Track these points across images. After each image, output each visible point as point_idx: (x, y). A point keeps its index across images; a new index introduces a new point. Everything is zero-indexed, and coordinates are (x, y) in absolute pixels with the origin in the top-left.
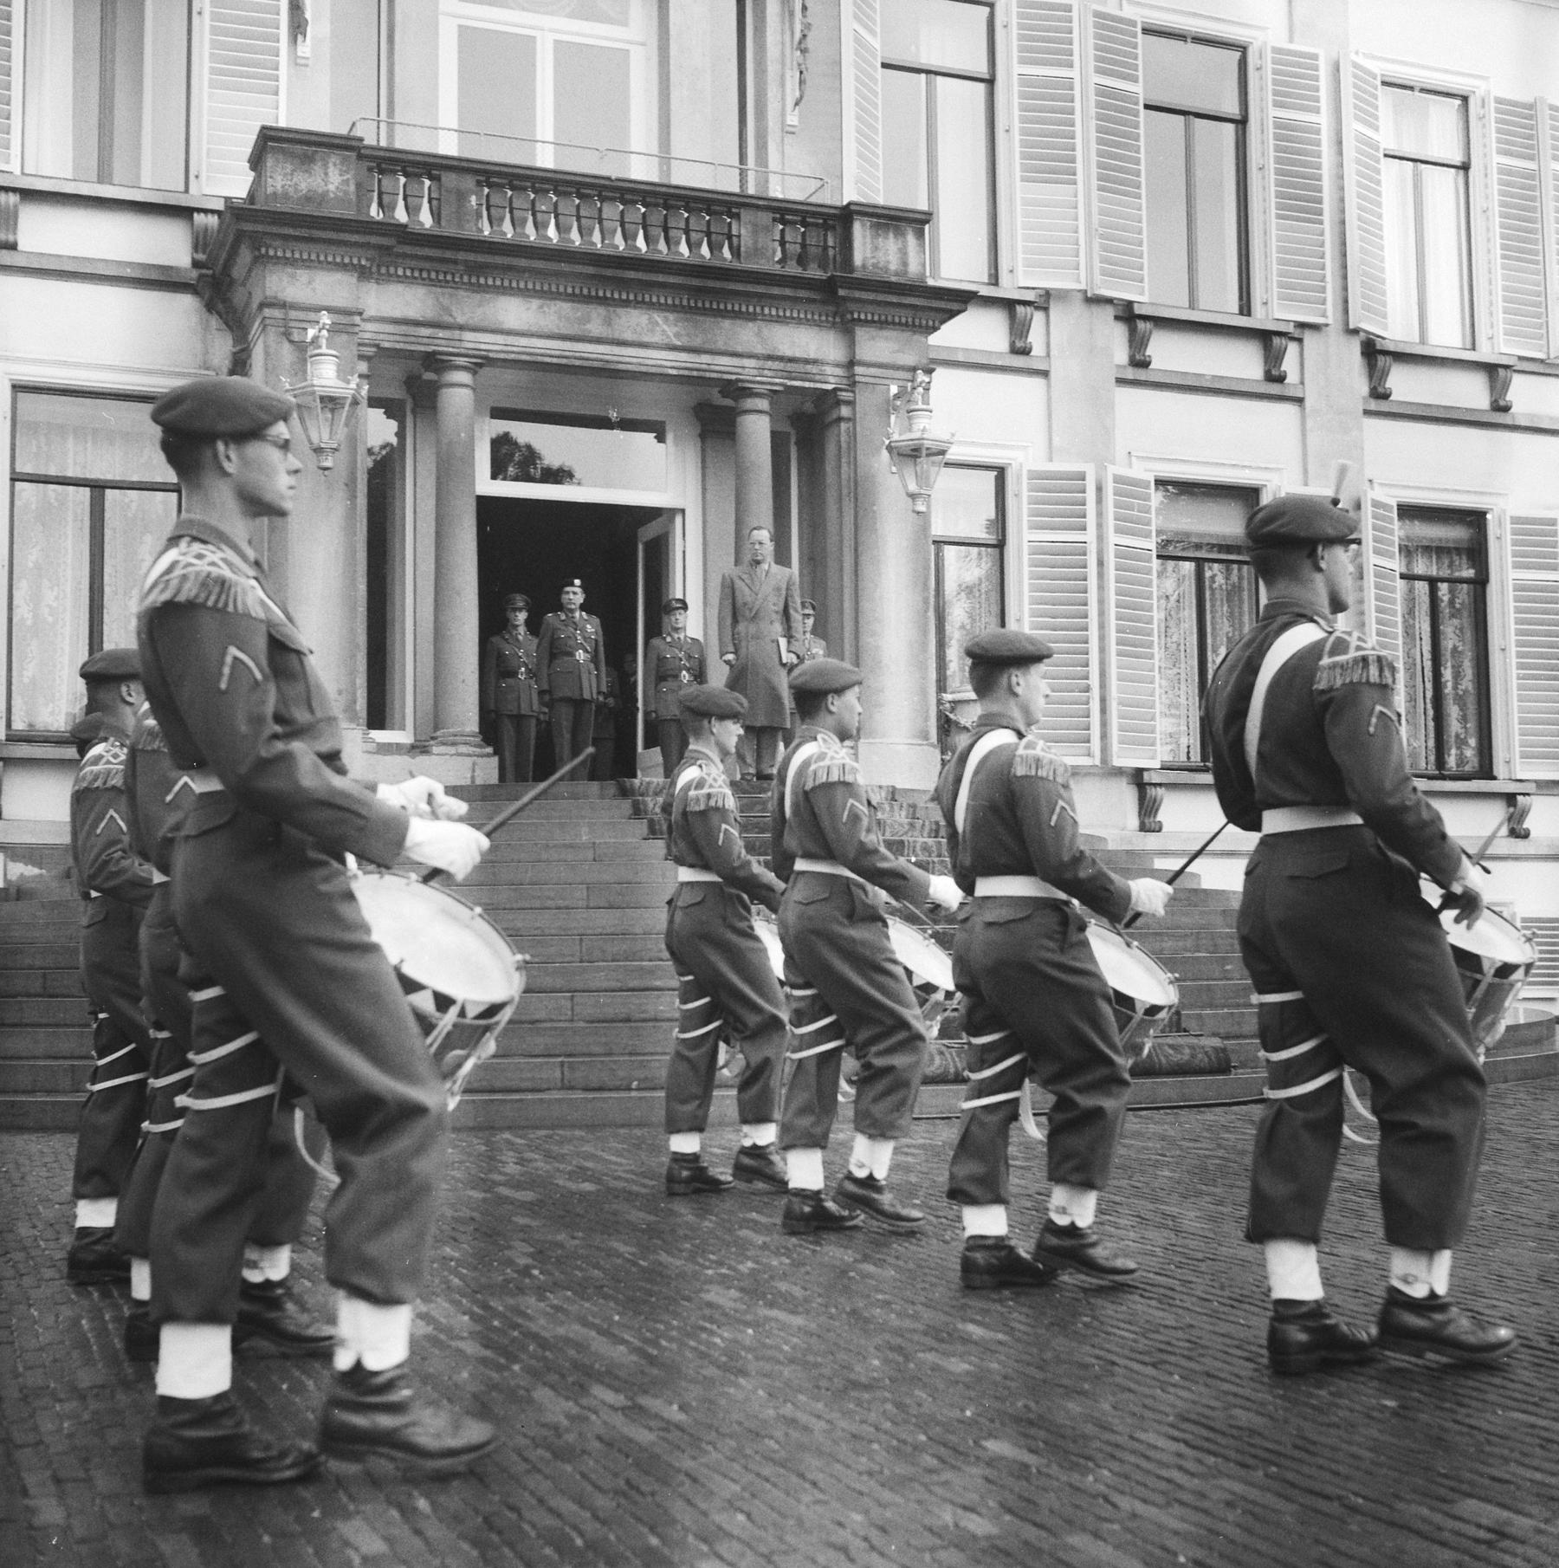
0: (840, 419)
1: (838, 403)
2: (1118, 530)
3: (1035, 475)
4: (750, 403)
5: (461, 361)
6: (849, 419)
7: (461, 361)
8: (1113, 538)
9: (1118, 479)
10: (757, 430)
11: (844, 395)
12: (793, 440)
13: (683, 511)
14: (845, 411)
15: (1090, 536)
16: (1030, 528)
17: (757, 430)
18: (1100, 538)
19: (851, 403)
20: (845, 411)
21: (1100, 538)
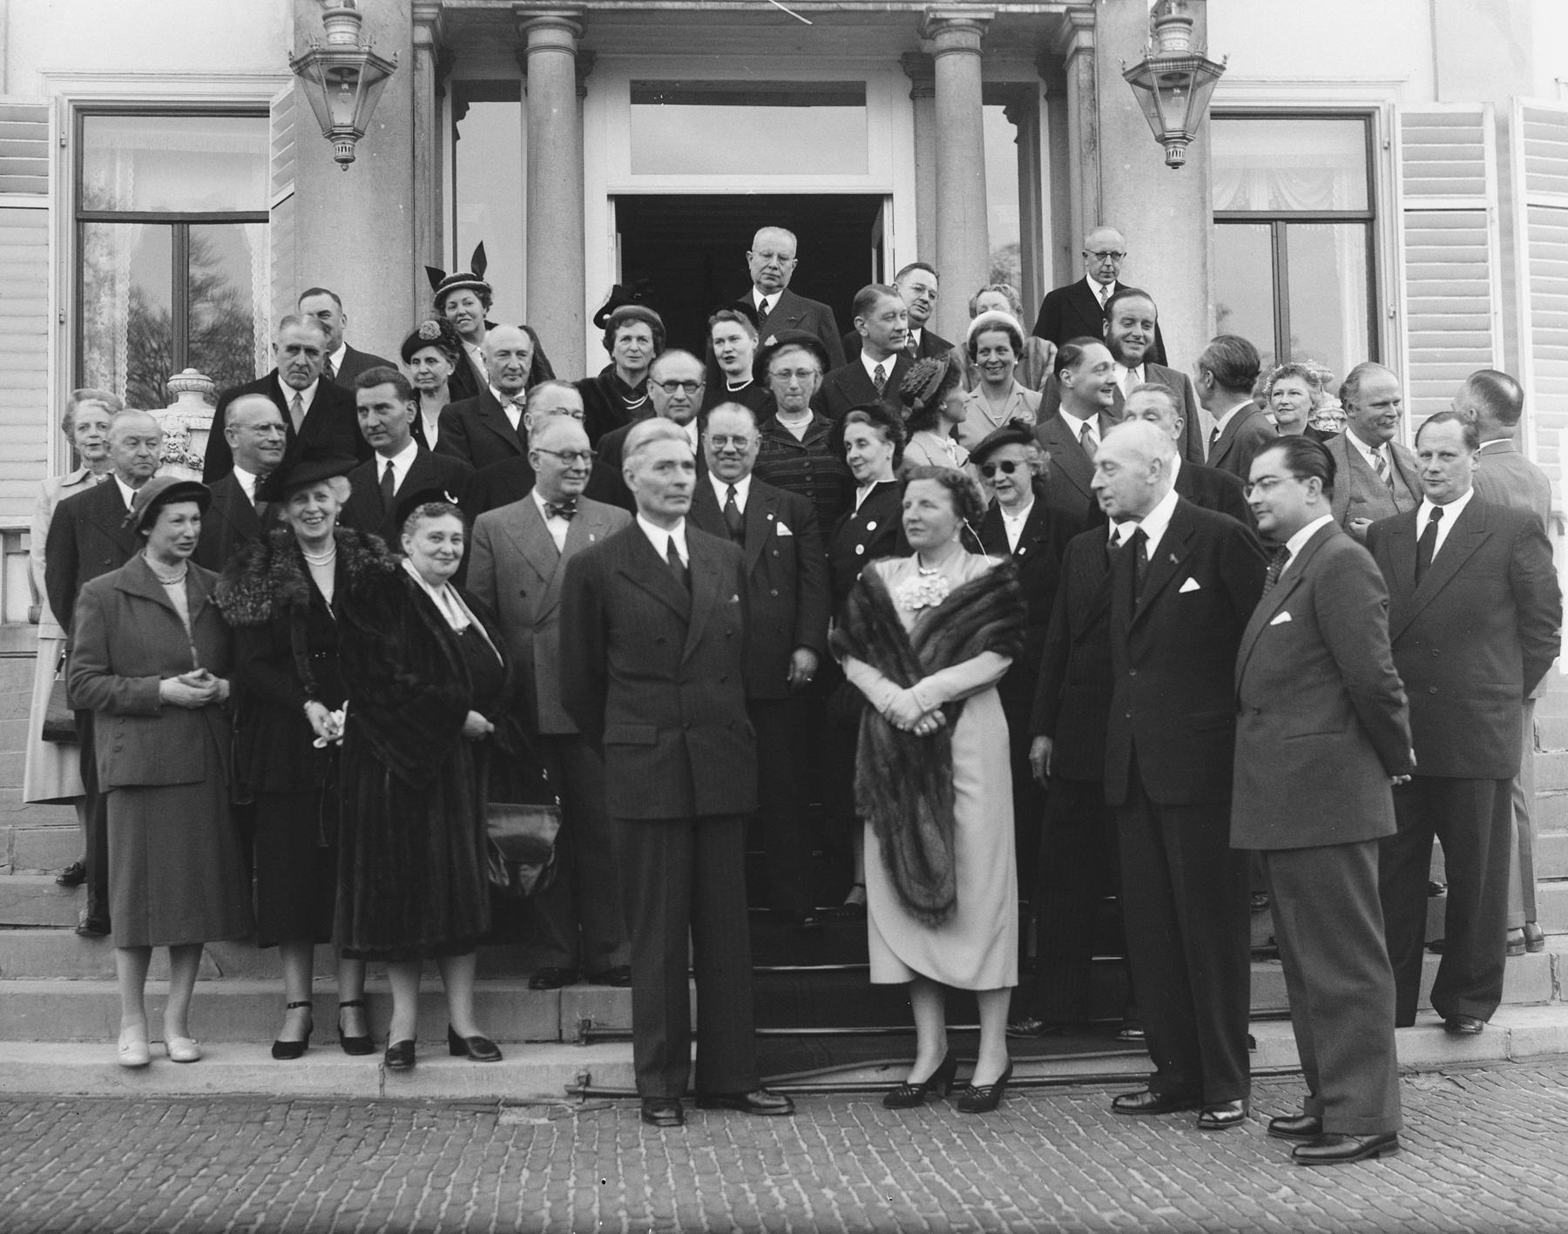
0: (1078, 50)
1: (1076, 28)
2: (1531, 187)
3: (1411, 120)
4: (946, 40)
5: (551, 16)
6: (1092, 51)
7: (551, 16)
8: (1523, 195)
9: (1529, 115)
10: (959, 74)
11: (1080, 18)
12: (1043, 90)
13: (890, 196)
14: (1084, 39)
15: (1490, 199)
16: (1406, 193)
17: (959, 74)
18: (1506, 199)
19: (1091, 27)
20: (1084, 39)
21: (1506, 199)
